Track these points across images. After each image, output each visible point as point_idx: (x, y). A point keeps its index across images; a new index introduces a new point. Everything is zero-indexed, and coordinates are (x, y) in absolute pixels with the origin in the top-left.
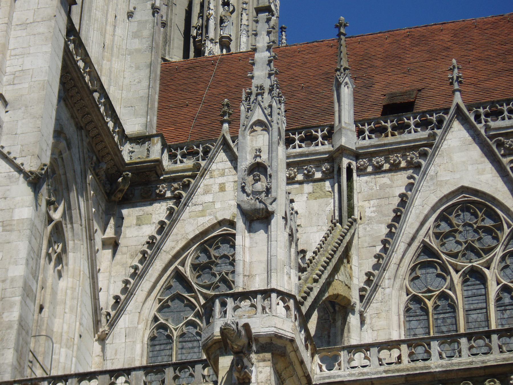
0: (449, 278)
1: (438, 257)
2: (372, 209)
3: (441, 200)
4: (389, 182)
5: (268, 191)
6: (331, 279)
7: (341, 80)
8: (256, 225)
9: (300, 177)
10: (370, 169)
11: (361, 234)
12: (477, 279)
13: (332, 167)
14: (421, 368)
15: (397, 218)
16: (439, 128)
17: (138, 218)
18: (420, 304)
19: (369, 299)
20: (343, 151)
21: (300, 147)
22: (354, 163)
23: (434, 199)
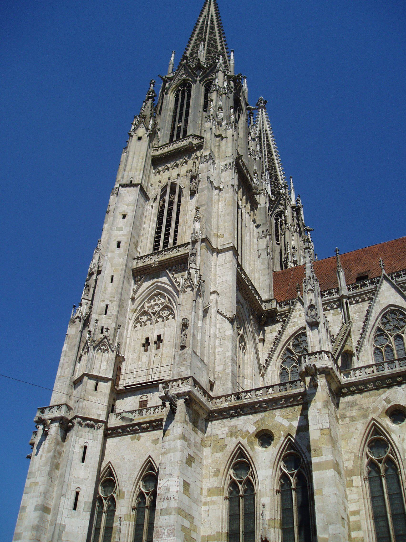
3: (382, 310)
4: (362, 306)
5: (316, 314)
7: (339, 270)
8: (313, 327)
9: (328, 308)
10: (354, 302)
11: (354, 327)
12: (399, 338)
13: (340, 303)
14: (382, 374)
15: (367, 319)
17: (271, 330)
20: (343, 296)
21: (327, 297)
23: (380, 310)
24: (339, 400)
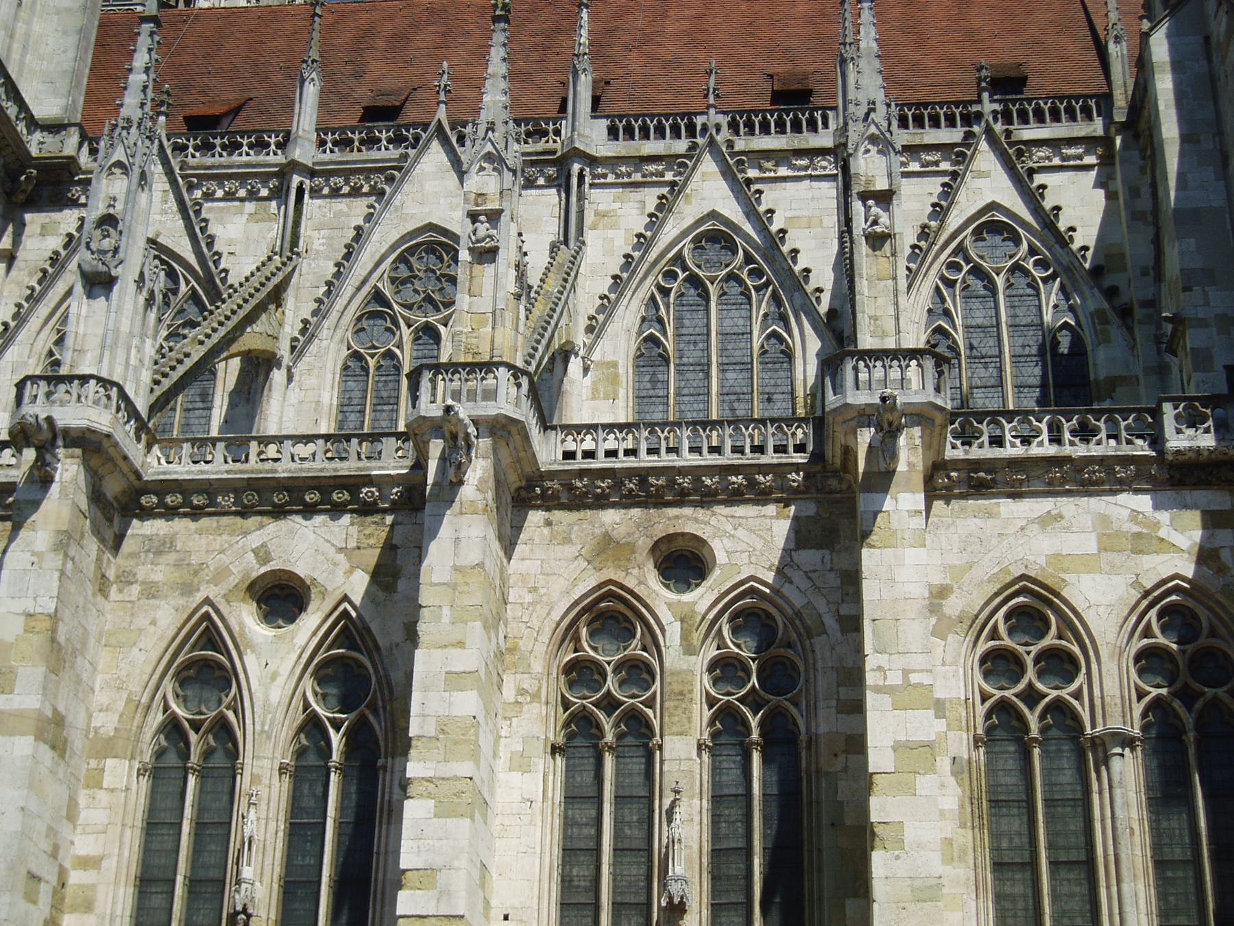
0: (398, 333)
1: (390, 307)
2: (321, 241)
4: (346, 209)
5: (116, 250)
6: (238, 334)
7: (306, 75)
8: (97, 290)
9: (242, 193)
10: (326, 191)
12: (430, 337)
13: (281, 184)
14: (267, 472)
15: (347, 256)
16: (414, 148)
17: (43, 227)
18: (361, 362)
19: (302, 352)
21: (248, 154)
22: (308, 182)
23: (395, 236)
24: (127, 526)
